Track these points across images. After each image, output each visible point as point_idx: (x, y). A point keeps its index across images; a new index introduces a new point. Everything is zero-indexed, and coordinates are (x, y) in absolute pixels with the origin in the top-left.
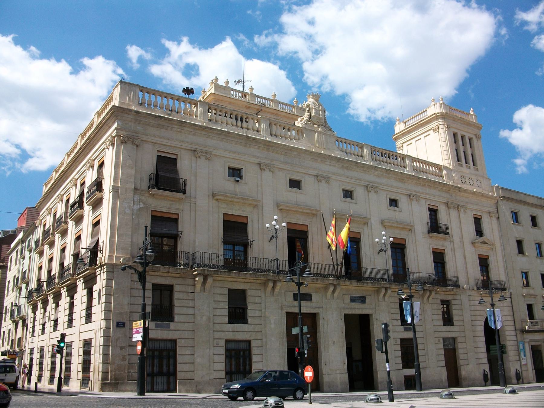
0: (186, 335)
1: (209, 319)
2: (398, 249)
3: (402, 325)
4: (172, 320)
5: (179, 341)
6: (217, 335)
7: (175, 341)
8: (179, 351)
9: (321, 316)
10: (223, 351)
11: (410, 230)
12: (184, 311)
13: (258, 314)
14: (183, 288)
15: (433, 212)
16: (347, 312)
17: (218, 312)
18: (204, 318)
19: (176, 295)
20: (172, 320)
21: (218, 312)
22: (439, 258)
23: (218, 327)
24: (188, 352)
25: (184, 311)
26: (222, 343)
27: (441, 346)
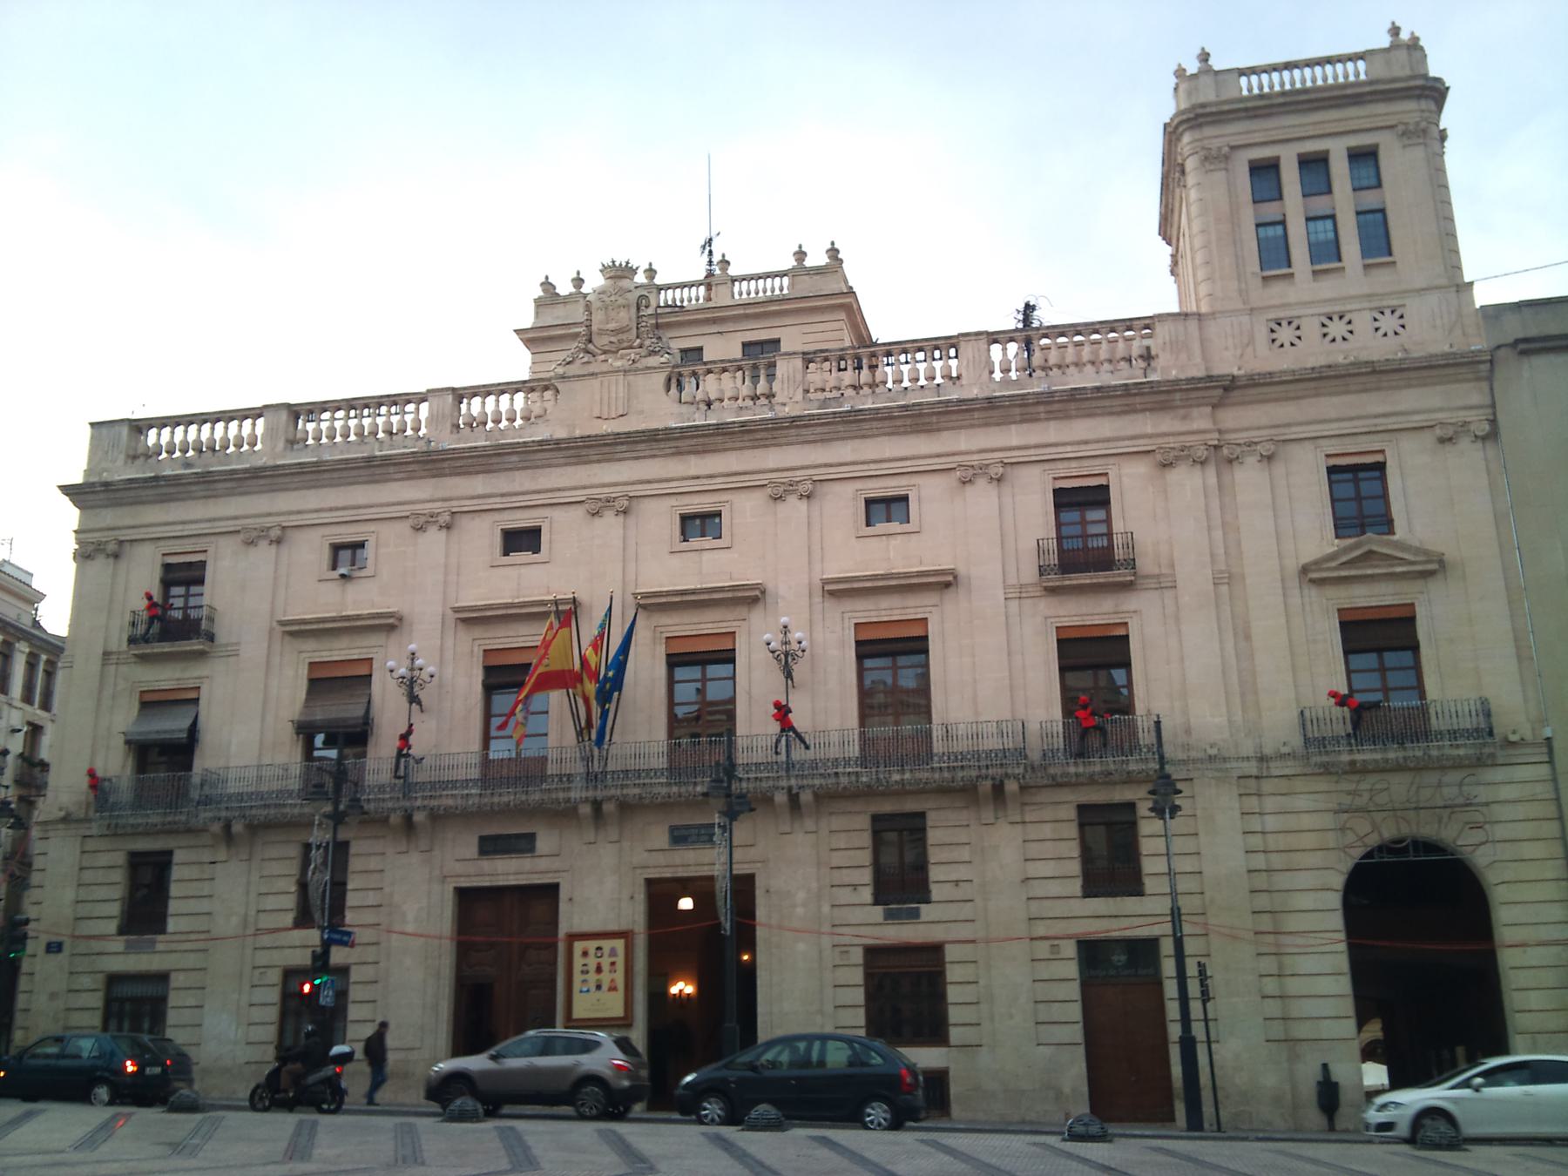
0: (191, 960)
1: (245, 923)
2: (893, 659)
3: (876, 903)
4: (163, 931)
5: (173, 976)
6: (263, 958)
7: (162, 978)
8: (174, 999)
9: (563, 894)
10: (274, 995)
11: (947, 585)
12: (192, 905)
13: (372, 898)
14: (191, 855)
15: (1081, 501)
16: (654, 874)
17: (271, 903)
18: (234, 920)
19: (176, 873)
20: (163, 931)
21: (271, 903)
22: (1093, 661)
23: (266, 940)
24: (191, 1001)
25: (192, 905)
26: (275, 977)
27: (1072, 970)
